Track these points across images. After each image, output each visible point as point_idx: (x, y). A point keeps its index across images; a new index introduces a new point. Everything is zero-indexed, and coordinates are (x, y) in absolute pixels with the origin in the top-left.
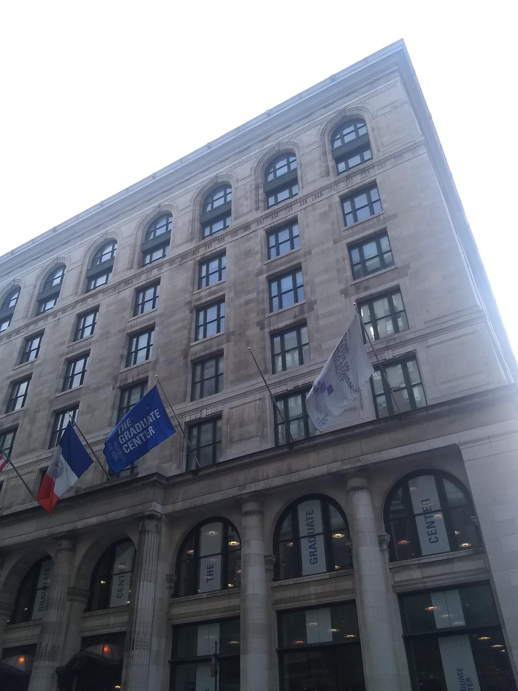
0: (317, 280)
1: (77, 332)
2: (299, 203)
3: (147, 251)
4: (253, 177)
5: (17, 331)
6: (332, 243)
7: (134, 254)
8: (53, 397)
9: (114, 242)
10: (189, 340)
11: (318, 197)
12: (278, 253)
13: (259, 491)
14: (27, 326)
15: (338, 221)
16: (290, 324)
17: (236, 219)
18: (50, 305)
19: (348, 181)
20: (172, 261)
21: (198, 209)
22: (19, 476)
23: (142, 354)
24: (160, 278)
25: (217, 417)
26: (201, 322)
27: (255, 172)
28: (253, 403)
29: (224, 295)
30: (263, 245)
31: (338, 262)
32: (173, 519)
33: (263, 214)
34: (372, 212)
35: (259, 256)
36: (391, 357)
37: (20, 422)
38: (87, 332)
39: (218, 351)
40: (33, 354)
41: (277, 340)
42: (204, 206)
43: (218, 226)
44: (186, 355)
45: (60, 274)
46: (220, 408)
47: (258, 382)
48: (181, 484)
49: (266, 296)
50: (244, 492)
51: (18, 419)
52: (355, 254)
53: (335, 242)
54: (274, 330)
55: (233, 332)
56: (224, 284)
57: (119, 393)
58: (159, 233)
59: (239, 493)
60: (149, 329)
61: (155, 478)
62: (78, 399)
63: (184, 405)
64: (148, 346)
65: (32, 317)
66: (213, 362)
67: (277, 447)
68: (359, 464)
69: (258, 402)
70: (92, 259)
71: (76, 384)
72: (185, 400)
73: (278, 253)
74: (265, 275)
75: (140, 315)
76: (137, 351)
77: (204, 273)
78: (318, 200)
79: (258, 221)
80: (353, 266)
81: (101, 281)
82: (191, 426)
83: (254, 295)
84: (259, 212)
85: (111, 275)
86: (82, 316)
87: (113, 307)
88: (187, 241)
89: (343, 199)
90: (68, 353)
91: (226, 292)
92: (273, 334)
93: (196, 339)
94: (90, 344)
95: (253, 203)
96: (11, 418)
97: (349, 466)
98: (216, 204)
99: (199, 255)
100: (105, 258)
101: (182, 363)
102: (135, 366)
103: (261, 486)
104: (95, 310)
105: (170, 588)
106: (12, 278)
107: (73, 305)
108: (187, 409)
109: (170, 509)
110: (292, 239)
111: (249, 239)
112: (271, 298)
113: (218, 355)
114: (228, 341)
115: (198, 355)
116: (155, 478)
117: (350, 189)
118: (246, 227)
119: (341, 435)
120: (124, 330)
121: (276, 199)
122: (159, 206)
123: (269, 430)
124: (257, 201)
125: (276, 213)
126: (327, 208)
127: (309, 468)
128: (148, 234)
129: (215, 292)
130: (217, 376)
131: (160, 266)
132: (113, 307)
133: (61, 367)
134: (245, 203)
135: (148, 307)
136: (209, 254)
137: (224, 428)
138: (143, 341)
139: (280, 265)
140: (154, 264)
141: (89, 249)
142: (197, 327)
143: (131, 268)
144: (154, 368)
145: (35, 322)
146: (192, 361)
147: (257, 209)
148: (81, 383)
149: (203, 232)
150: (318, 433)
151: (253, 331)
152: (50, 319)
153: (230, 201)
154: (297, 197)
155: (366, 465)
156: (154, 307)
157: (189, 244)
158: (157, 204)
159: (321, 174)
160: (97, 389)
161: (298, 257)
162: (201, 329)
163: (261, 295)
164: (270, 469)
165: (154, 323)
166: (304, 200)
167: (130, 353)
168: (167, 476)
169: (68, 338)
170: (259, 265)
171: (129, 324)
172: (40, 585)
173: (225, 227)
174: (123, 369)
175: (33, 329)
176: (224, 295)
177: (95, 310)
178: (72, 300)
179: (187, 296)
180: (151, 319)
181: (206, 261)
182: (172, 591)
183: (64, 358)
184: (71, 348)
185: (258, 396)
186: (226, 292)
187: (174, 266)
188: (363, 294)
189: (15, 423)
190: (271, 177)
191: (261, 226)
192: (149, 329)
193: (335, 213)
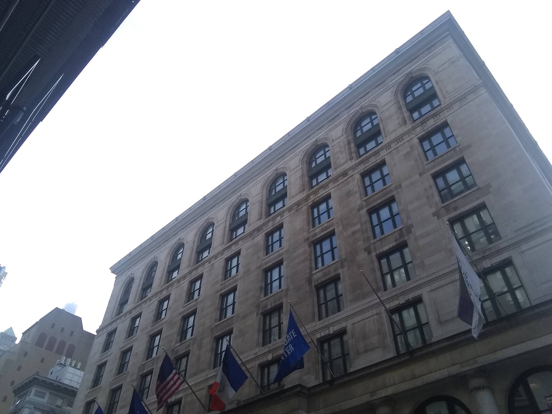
0: (410, 207)
1: (227, 272)
2: (385, 150)
4: (345, 136)
5: (184, 277)
6: (418, 176)
7: (262, 207)
8: (213, 326)
9: (247, 201)
11: (400, 142)
12: (373, 190)
13: (389, 396)
14: (190, 272)
15: (421, 159)
16: (393, 247)
17: (335, 169)
18: (206, 254)
19: (423, 125)
20: (290, 209)
21: (305, 166)
22: (194, 393)
23: (276, 284)
24: (283, 223)
25: (342, 333)
26: (319, 253)
27: (346, 132)
28: (372, 318)
29: (334, 230)
30: (360, 185)
31: (426, 190)
33: (357, 162)
34: (448, 146)
35: (358, 195)
36: (489, 265)
37: (191, 348)
38: (234, 271)
39: (336, 275)
40: (196, 293)
41: (384, 261)
42: (310, 163)
43: (322, 177)
44: (310, 281)
45: (211, 230)
46: (344, 325)
47: (373, 299)
49: (369, 225)
50: (376, 397)
51: (189, 346)
52: (440, 181)
53: (421, 175)
54: (380, 253)
55: (346, 259)
56: (333, 221)
58: (278, 189)
59: (372, 399)
60: (279, 264)
61: (299, 389)
62: (232, 326)
63: (314, 324)
64: (280, 278)
65: (194, 265)
66: (333, 286)
67: (399, 355)
69: (375, 317)
71: (229, 314)
72: (314, 320)
73: (373, 190)
74: (365, 209)
75: (271, 254)
76: (272, 282)
77: (316, 215)
78: (400, 144)
79: (353, 168)
80: (440, 192)
81: (240, 231)
82: (322, 341)
83: (358, 227)
84: (353, 161)
85: (247, 226)
86: (229, 260)
88: (300, 192)
89: (422, 140)
90: (221, 290)
91: (335, 227)
92: (380, 257)
93: (316, 268)
94: (236, 281)
95: (348, 155)
96: (185, 345)
97: (467, 368)
98: (319, 161)
99: (310, 201)
100: (242, 214)
101: (308, 289)
102: (272, 295)
103: (390, 391)
104: (238, 254)
106: (178, 238)
108: (317, 327)
110: (383, 178)
111: (348, 183)
112: (373, 227)
113: (336, 279)
114: (342, 266)
115: (320, 281)
116: (299, 389)
117: (426, 131)
118: (345, 174)
119: (455, 340)
121: (365, 149)
122: (276, 170)
123: (389, 340)
124: (350, 154)
125: (368, 159)
126: (409, 149)
127: (431, 372)
128: (270, 191)
129: (327, 228)
130: (338, 297)
131: (281, 214)
133: (217, 301)
134: (341, 156)
135: (276, 246)
136: (317, 199)
137: (350, 341)
138: (275, 274)
139: (377, 200)
140: (277, 213)
142: (316, 258)
143: (261, 218)
144: (286, 295)
145: (196, 269)
146: (315, 286)
147: (351, 159)
148: (233, 313)
149: (311, 183)
150: (434, 340)
151: (362, 256)
152: (207, 265)
153: (329, 157)
154: (382, 144)
155: (483, 366)
156: (280, 246)
157: (302, 194)
158: (274, 168)
159: (399, 124)
160: (245, 317)
161: (391, 191)
162: (320, 259)
163: (364, 226)
165: (282, 259)
166: (389, 145)
167: (266, 285)
168: (308, 387)
169: (220, 277)
170: (359, 202)
171: (264, 262)
173: (328, 177)
174: (263, 298)
175: (195, 274)
176: (334, 230)
177: (238, 254)
178: (220, 249)
179: (305, 234)
180: (280, 255)
181: (316, 205)
183: (219, 294)
184: (223, 286)
185: (375, 311)
186: (335, 227)
187: (292, 212)
189: (187, 349)
190: (359, 134)
191: (356, 172)
192: (279, 264)
193: (416, 152)
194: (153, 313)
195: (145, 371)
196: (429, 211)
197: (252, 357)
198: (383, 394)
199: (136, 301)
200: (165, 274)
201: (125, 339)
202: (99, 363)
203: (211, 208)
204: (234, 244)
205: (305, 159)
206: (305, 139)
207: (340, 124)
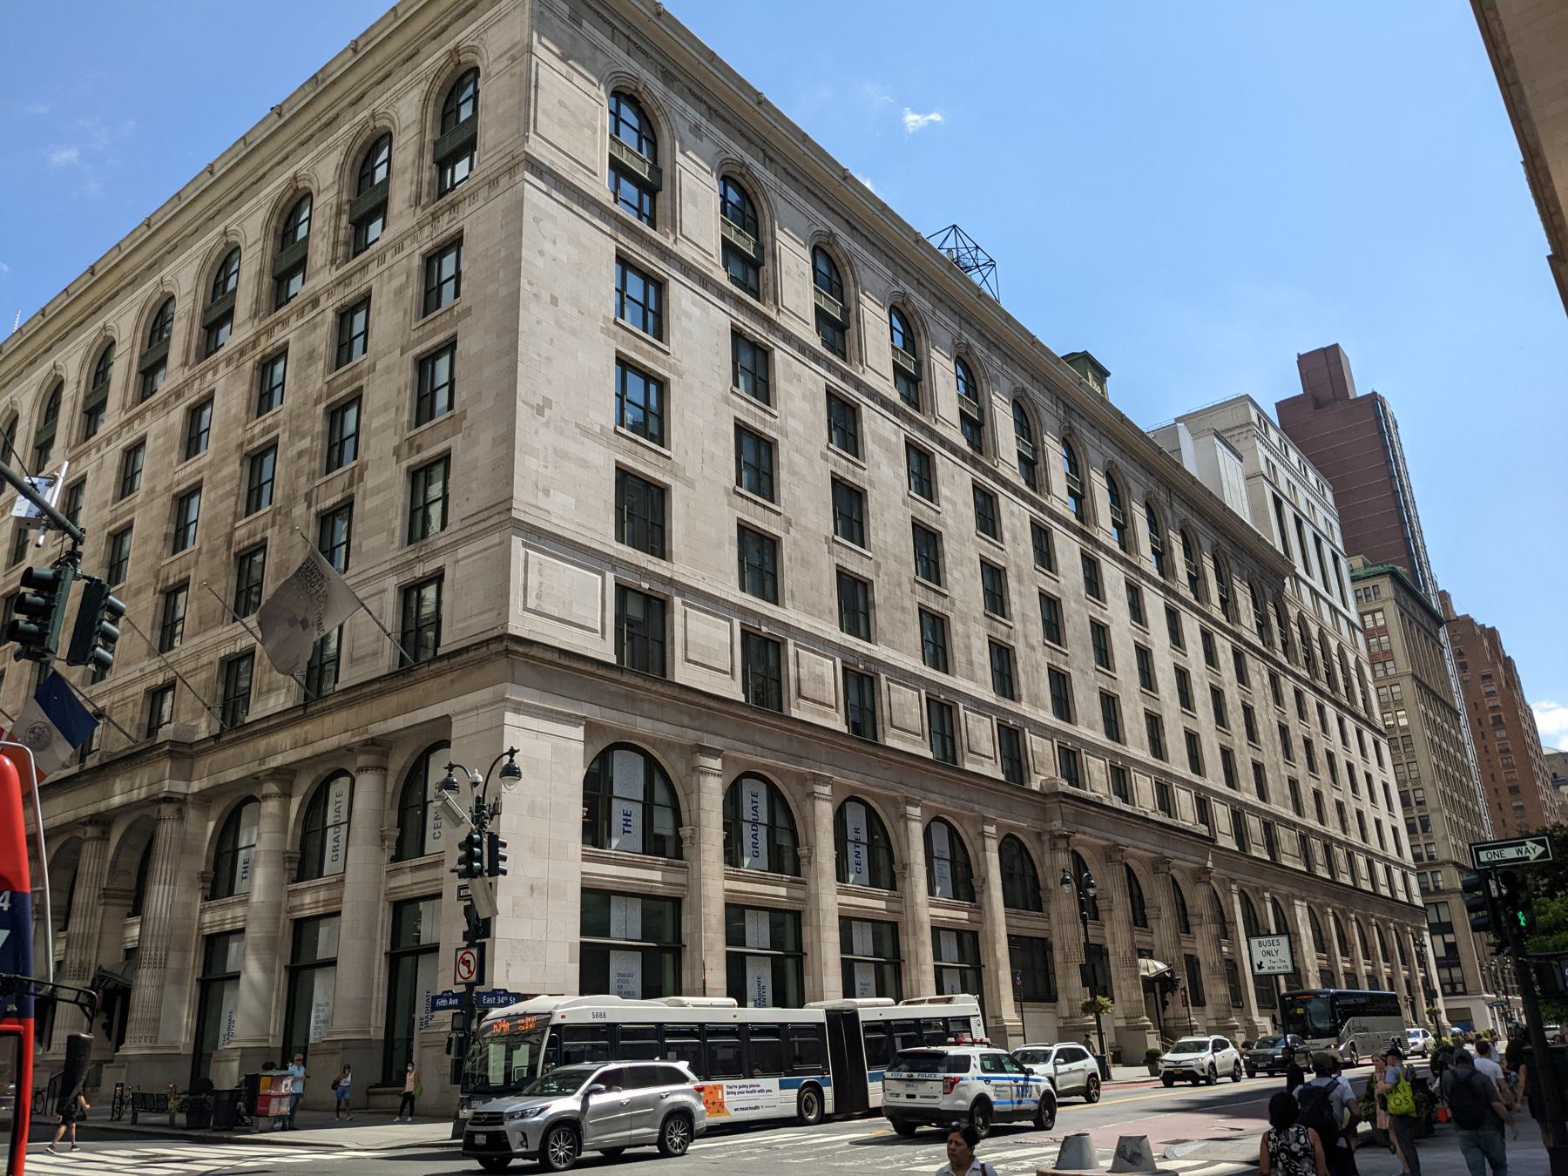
3: (444, 162)
7: (190, 333)
10: (236, 517)
32: (205, 799)
48: (205, 752)
49: (320, 445)
57: (162, 601)
68: (366, 737)
70: (148, 332)
74: (323, 405)
87: (161, 441)
91: (280, 430)
107: (413, 234)
109: (196, 786)
111: (315, 327)
114: (273, 525)
132: (161, 441)
141: (142, 313)
146: (236, 555)
151: (300, 509)
164: (283, 738)
171: (176, 477)
172: (243, 843)
179: (240, 430)
180: (199, 471)
188: (415, 459)
194: (7, 546)
197: (138, 674)
199: (129, 404)
200: (133, 378)
203: (110, 299)
204: (152, 408)
205: (273, 223)
206: (279, 163)
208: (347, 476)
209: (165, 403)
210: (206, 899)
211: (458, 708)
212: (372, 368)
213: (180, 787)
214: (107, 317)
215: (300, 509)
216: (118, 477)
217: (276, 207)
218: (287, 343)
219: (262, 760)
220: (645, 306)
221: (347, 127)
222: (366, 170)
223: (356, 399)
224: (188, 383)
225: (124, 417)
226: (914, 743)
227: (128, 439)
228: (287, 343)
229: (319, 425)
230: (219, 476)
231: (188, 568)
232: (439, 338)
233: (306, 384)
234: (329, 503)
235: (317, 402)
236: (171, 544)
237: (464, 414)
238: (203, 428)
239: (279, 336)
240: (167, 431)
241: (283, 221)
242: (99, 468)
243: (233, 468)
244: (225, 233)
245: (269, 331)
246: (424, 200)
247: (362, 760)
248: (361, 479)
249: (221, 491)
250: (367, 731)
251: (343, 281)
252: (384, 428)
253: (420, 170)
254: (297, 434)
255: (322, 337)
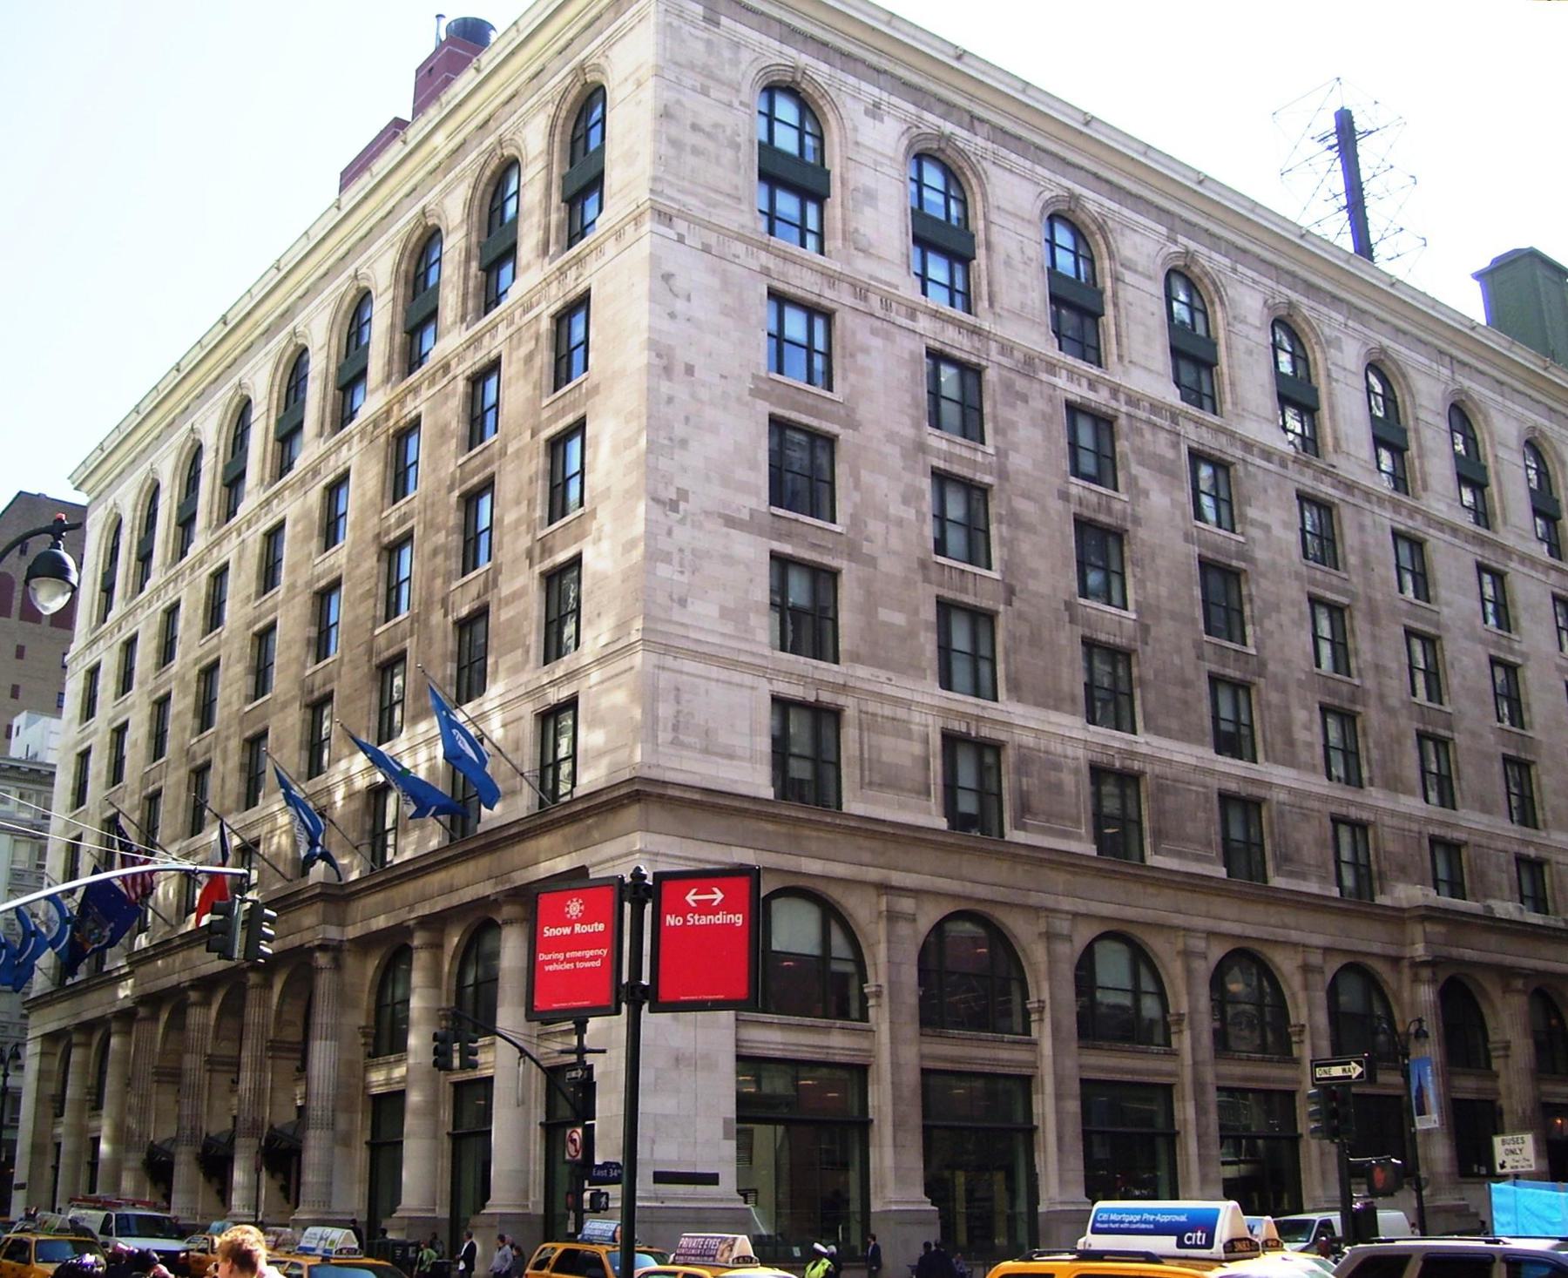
29: (412, 529)
32: (367, 943)
44: (370, 652)
49: (456, 541)
68: (507, 886)
74: (456, 493)
87: (299, 528)
105: (365, 1044)
109: (353, 932)
111: (447, 397)
120: (309, 584)
141: (276, 369)
151: (437, 617)
170: (452, 469)
176: (412, 529)
179: (376, 520)
182: (371, 1049)
188: (548, 564)
195: (150, 789)
196: (525, 542)
198: (424, 910)
201: (116, 698)
202: (80, 749)
205: (403, 267)
207: (459, 179)
208: (482, 578)
209: (302, 481)
210: (369, 1056)
211: (595, 860)
212: (503, 453)
213: (333, 933)
214: (243, 373)
215: (437, 617)
216: (260, 567)
217: (405, 247)
218: (419, 417)
219: (412, 907)
220: (810, 349)
221: (474, 154)
222: (497, 203)
223: (488, 485)
224: (324, 457)
225: (263, 497)
226: (1198, 858)
227: (267, 524)
228: (419, 417)
229: (454, 518)
230: (358, 572)
231: (331, 681)
232: (569, 419)
233: (439, 464)
234: (464, 611)
235: (451, 489)
236: (313, 650)
237: (594, 512)
238: (340, 512)
239: (413, 406)
240: (306, 514)
241: (414, 262)
242: (240, 557)
243: (370, 563)
244: (356, 276)
245: (401, 401)
246: (552, 250)
247: (508, 911)
248: (495, 581)
249: (359, 592)
250: (509, 881)
251: (475, 342)
252: (518, 522)
253: (547, 212)
254: (430, 526)
255: (452, 412)
